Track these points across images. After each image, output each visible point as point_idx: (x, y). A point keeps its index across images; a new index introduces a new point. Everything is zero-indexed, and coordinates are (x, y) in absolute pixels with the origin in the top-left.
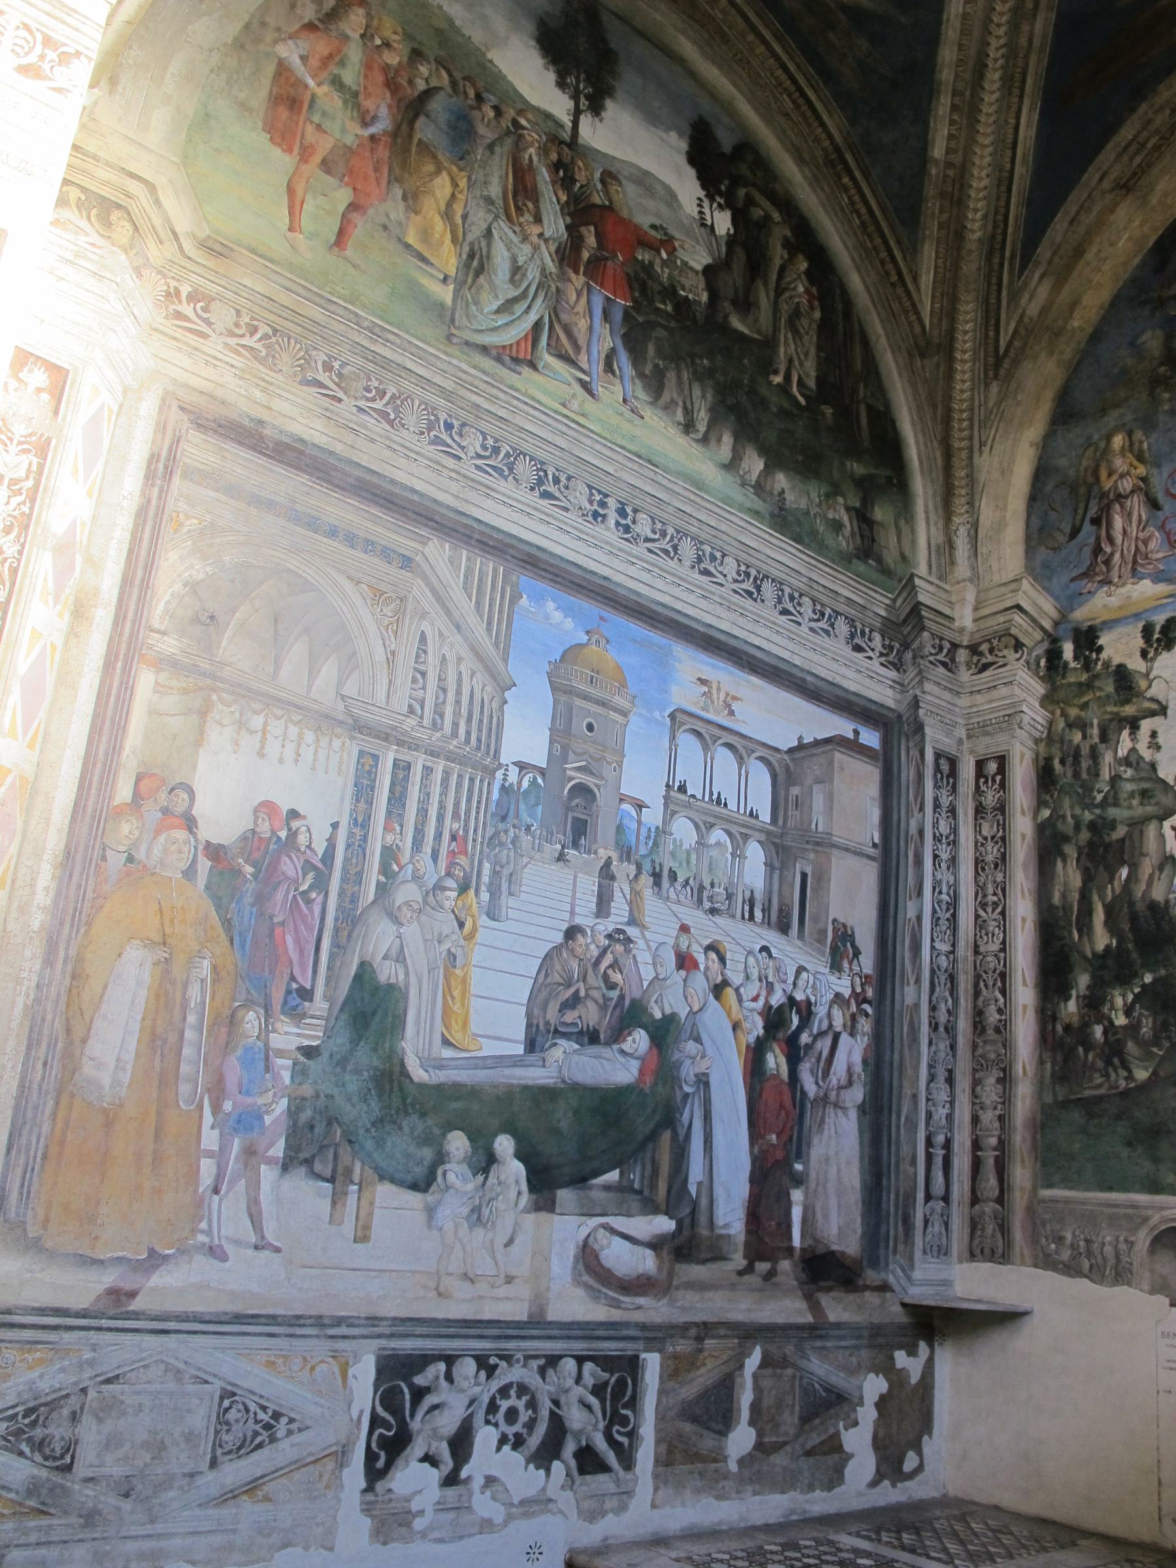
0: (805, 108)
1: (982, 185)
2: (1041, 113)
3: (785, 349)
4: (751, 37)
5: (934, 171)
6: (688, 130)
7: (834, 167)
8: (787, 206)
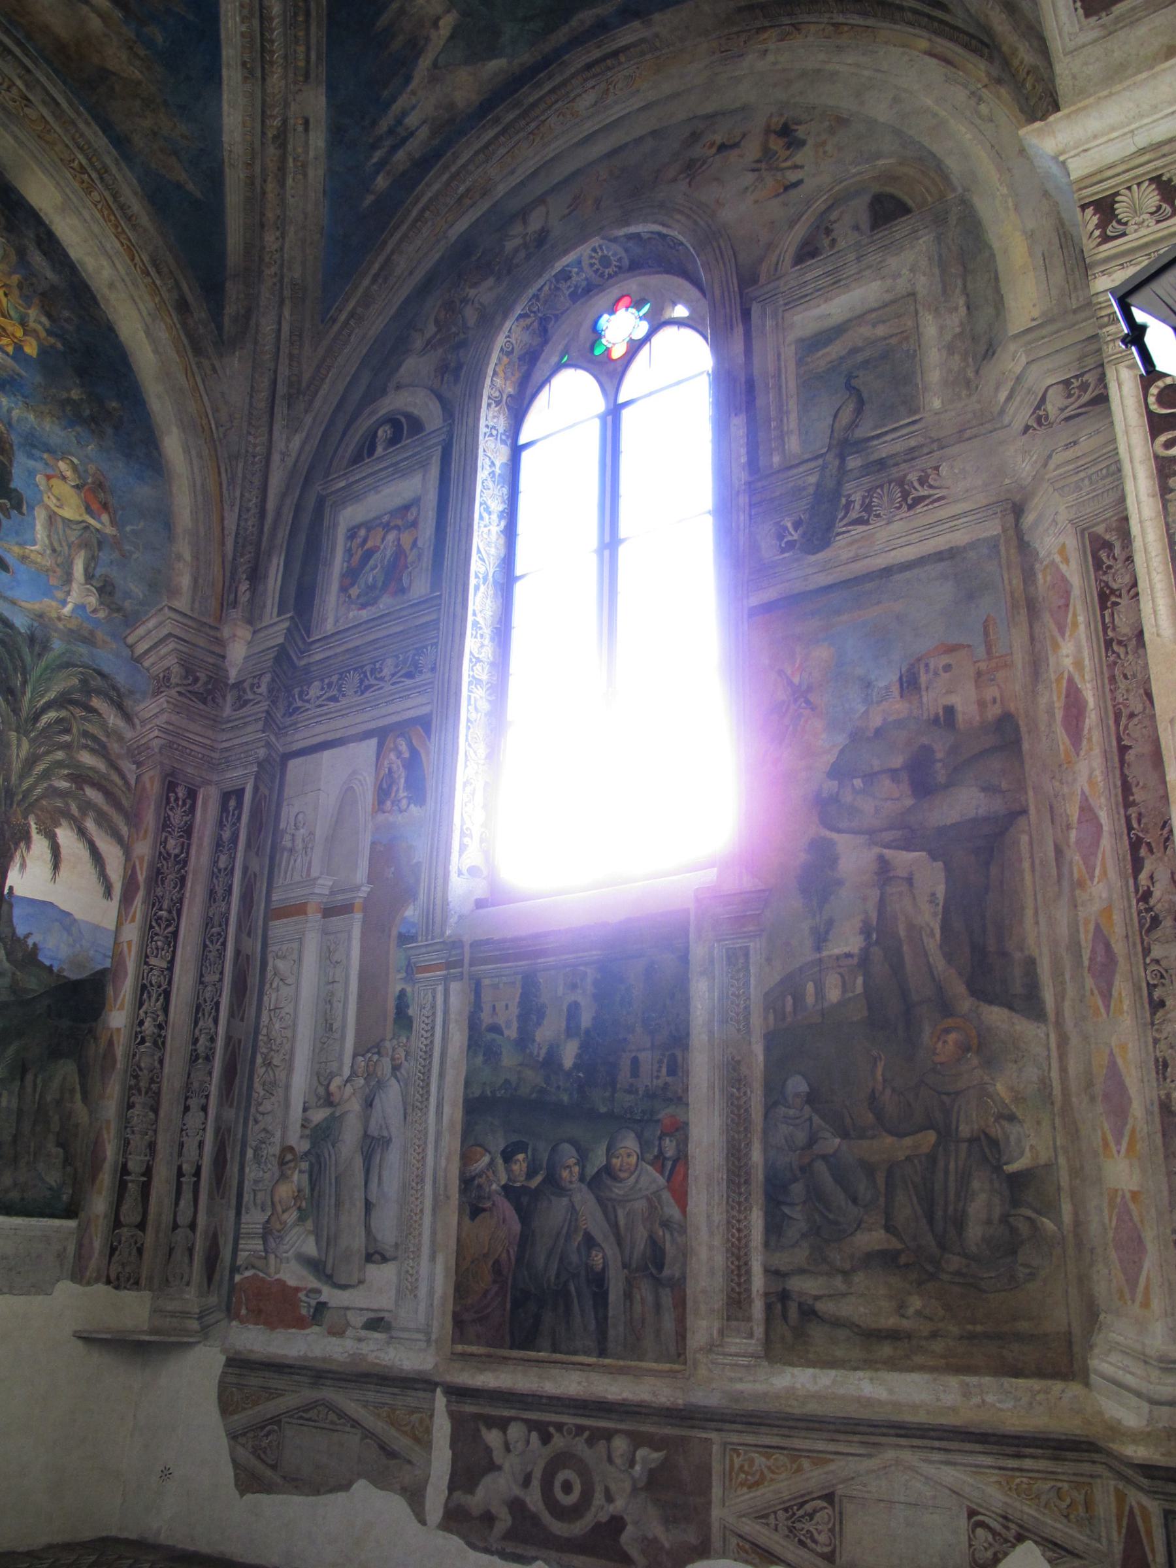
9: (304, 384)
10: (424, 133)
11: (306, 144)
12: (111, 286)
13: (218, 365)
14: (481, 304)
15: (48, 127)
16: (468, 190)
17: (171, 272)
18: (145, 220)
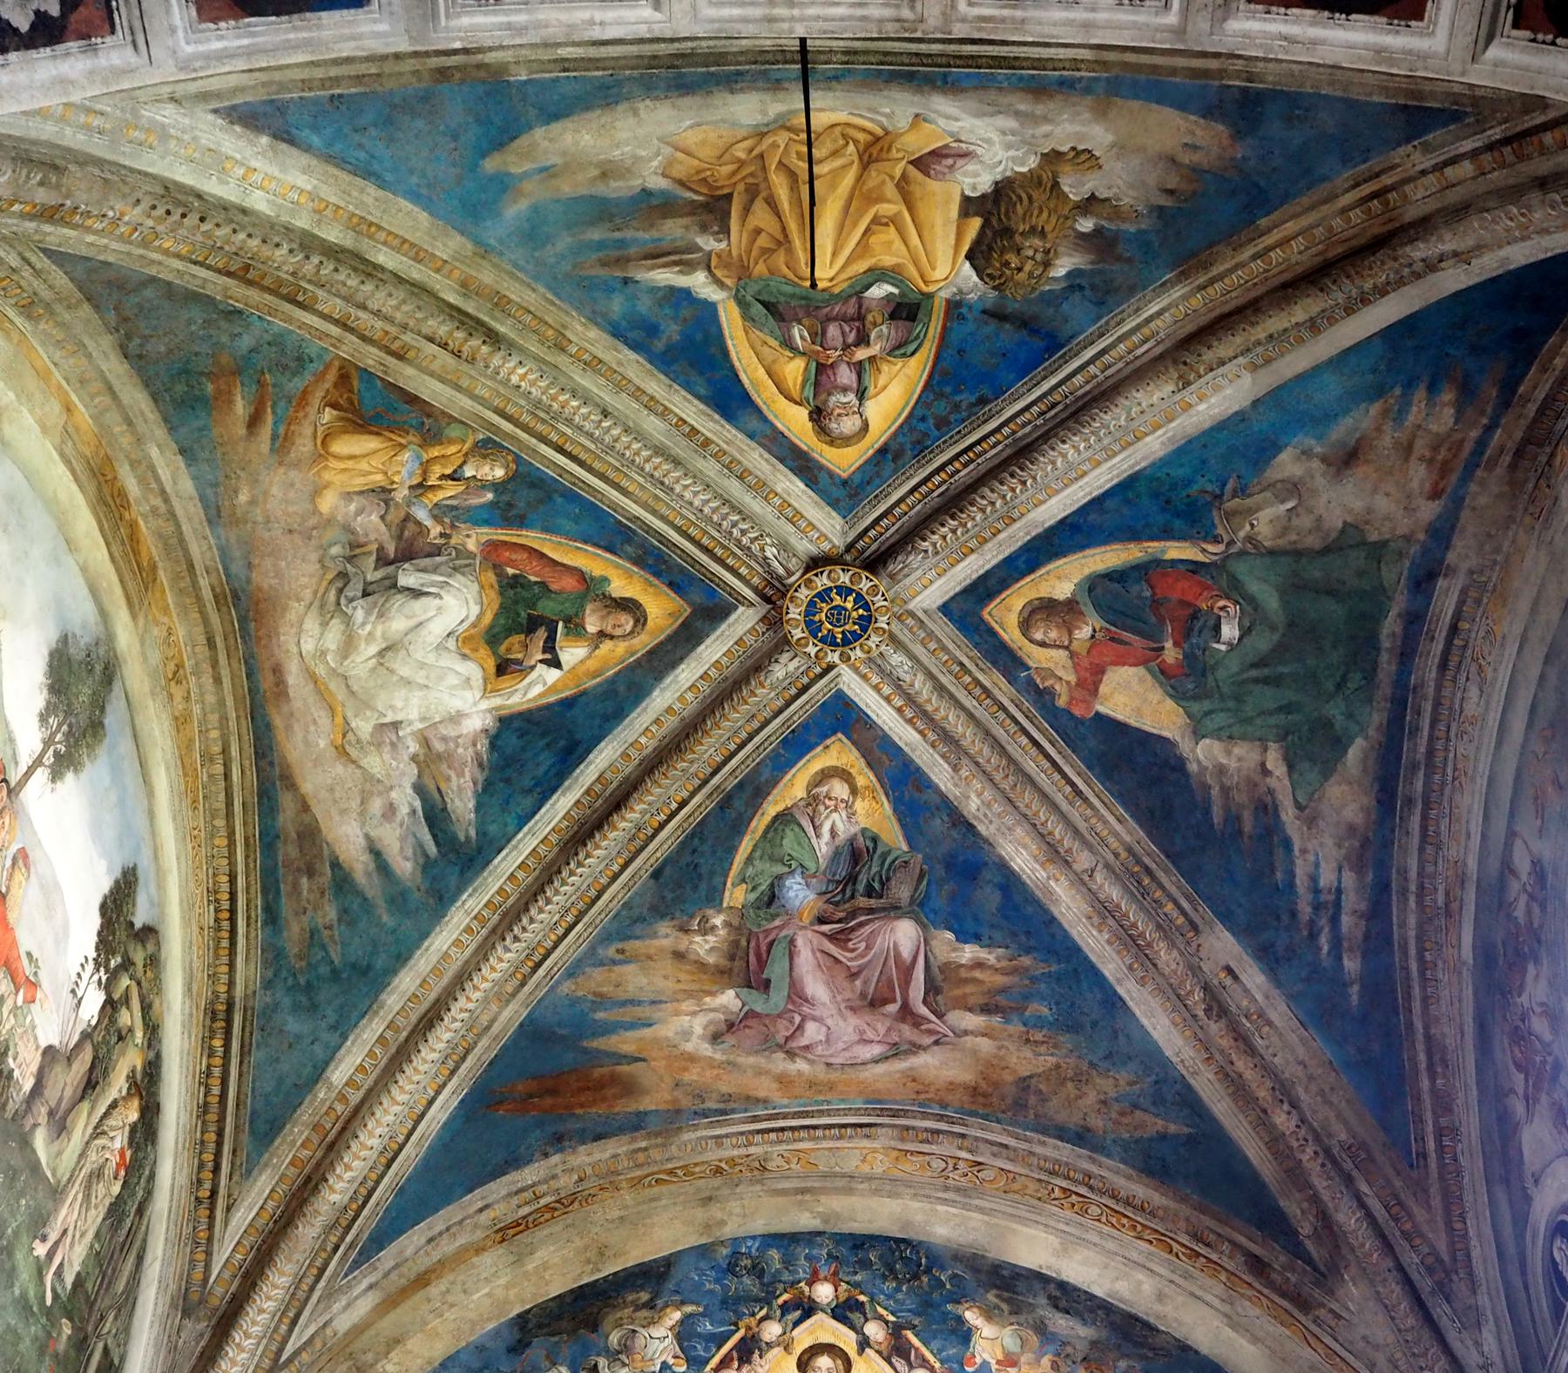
0: (226, 935)
1: (370, 1143)
2: (462, 1101)
3: (67, 1215)
4: (220, 823)
5: (321, 1095)
6: (118, 873)
7: (213, 1019)
8: (153, 1030)
9: (1446, 1257)
10: (1349, 879)
11: (1246, 991)
12: (1160, 1297)
13: (1335, 1306)
14: (1542, 1004)
15: (1011, 1176)
16: (1447, 894)
17: (1219, 1235)
18: (1157, 1199)
